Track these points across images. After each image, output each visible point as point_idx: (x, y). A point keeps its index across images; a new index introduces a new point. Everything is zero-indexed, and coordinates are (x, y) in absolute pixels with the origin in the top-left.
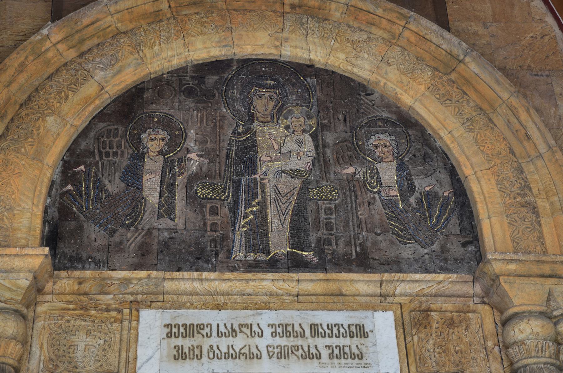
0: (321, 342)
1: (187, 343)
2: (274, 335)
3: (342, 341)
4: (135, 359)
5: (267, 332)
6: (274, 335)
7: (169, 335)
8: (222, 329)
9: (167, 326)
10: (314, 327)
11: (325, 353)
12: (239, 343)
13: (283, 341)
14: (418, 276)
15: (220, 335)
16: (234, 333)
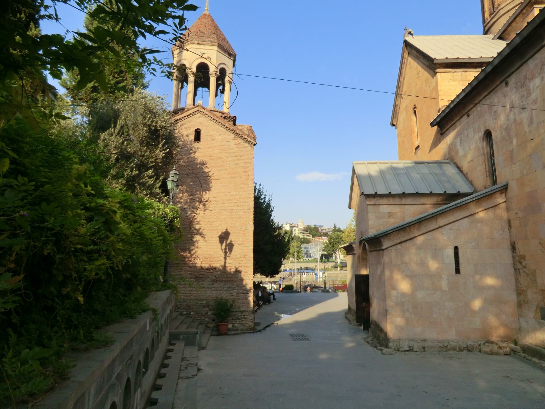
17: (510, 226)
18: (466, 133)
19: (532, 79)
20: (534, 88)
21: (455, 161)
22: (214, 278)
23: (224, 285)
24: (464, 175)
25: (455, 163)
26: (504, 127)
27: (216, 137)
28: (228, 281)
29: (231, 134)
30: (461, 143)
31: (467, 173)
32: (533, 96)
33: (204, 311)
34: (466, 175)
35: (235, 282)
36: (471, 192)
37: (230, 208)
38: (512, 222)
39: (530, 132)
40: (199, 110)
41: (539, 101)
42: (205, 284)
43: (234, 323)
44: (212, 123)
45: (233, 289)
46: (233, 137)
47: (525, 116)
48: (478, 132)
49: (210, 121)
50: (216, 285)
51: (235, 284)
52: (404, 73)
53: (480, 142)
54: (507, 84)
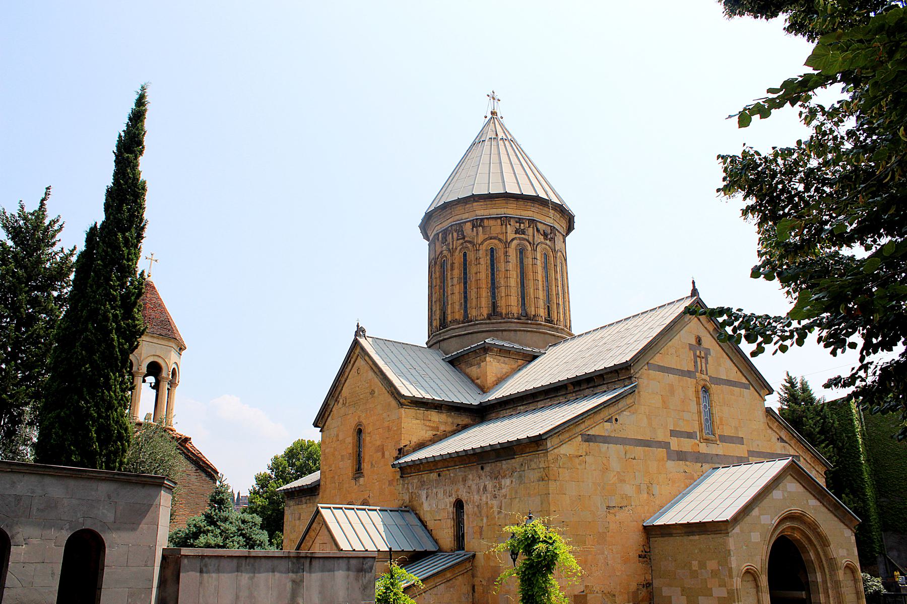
17: (474, 591)
18: (435, 490)
19: (504, 477)
20: (505, 485)
21: (418, 512)
24: (428, 530)
25: (416, 514)
26: (477, 504)
29: (193, 466)
30: (427, 498)
31: (431, 530)
32: (503, 491)
34: (430, 531)
36: (435, 550)
38: (476, 588)
39: (498, 518)
41: (507, 497)
47: (495, 503)
48: (450, 496)
52: (347, 374)
53: (450, 507)
54: (482, 468)
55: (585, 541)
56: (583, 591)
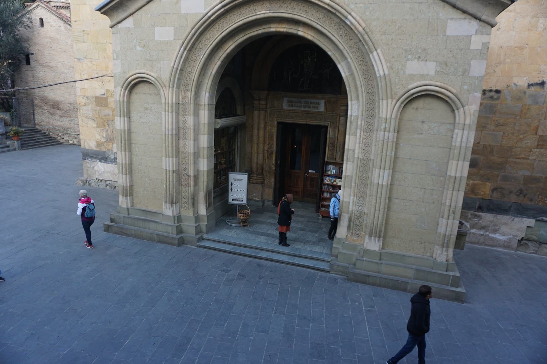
0: (312, 105)
1: (291, 104)
2: (304, 103)
3: (315, 105)
4: (283, 106)
5: (303, 103)
6: (304, 103)
7: (288, 102)
8: (296, 102)
9: (288, 101)
10: (311, 102)
11: (312, 107)
12: (299, 104)
13: (305, 105)
14: (329, 95)
15: (296, 103)
16: (298, 103)
22: (60, 114)
23: (66, 119)
27: (53, 24)
28: (68, 117)
29: (61, 21)
33: (57, 133)
35: (72, 117)
37: (65, 72)
40: (39, 4)
42: (56, 117)
43: (73, 141)
44: (49, 13)
45: (72, 121)
46: (63, 23)
49: (47, 12)
50: (62, 119)
51: (72, 118)
55: (105, 49)
56: (104, 94)
